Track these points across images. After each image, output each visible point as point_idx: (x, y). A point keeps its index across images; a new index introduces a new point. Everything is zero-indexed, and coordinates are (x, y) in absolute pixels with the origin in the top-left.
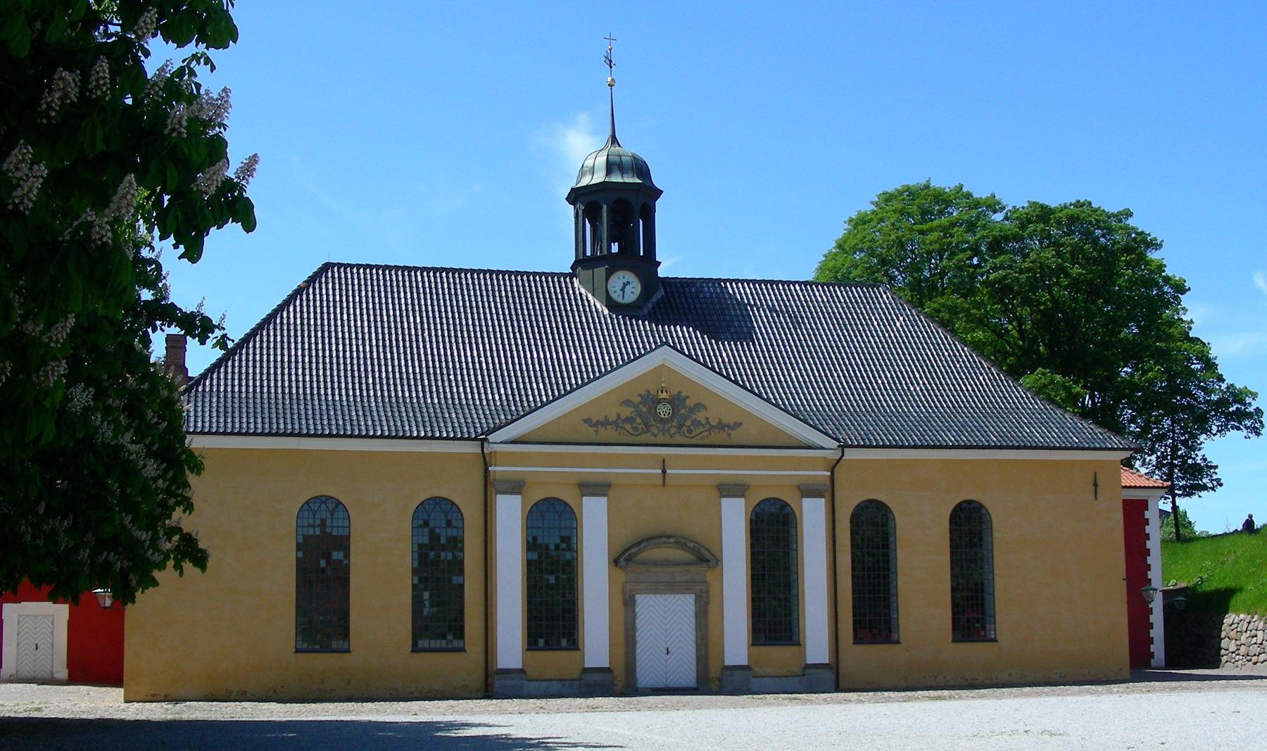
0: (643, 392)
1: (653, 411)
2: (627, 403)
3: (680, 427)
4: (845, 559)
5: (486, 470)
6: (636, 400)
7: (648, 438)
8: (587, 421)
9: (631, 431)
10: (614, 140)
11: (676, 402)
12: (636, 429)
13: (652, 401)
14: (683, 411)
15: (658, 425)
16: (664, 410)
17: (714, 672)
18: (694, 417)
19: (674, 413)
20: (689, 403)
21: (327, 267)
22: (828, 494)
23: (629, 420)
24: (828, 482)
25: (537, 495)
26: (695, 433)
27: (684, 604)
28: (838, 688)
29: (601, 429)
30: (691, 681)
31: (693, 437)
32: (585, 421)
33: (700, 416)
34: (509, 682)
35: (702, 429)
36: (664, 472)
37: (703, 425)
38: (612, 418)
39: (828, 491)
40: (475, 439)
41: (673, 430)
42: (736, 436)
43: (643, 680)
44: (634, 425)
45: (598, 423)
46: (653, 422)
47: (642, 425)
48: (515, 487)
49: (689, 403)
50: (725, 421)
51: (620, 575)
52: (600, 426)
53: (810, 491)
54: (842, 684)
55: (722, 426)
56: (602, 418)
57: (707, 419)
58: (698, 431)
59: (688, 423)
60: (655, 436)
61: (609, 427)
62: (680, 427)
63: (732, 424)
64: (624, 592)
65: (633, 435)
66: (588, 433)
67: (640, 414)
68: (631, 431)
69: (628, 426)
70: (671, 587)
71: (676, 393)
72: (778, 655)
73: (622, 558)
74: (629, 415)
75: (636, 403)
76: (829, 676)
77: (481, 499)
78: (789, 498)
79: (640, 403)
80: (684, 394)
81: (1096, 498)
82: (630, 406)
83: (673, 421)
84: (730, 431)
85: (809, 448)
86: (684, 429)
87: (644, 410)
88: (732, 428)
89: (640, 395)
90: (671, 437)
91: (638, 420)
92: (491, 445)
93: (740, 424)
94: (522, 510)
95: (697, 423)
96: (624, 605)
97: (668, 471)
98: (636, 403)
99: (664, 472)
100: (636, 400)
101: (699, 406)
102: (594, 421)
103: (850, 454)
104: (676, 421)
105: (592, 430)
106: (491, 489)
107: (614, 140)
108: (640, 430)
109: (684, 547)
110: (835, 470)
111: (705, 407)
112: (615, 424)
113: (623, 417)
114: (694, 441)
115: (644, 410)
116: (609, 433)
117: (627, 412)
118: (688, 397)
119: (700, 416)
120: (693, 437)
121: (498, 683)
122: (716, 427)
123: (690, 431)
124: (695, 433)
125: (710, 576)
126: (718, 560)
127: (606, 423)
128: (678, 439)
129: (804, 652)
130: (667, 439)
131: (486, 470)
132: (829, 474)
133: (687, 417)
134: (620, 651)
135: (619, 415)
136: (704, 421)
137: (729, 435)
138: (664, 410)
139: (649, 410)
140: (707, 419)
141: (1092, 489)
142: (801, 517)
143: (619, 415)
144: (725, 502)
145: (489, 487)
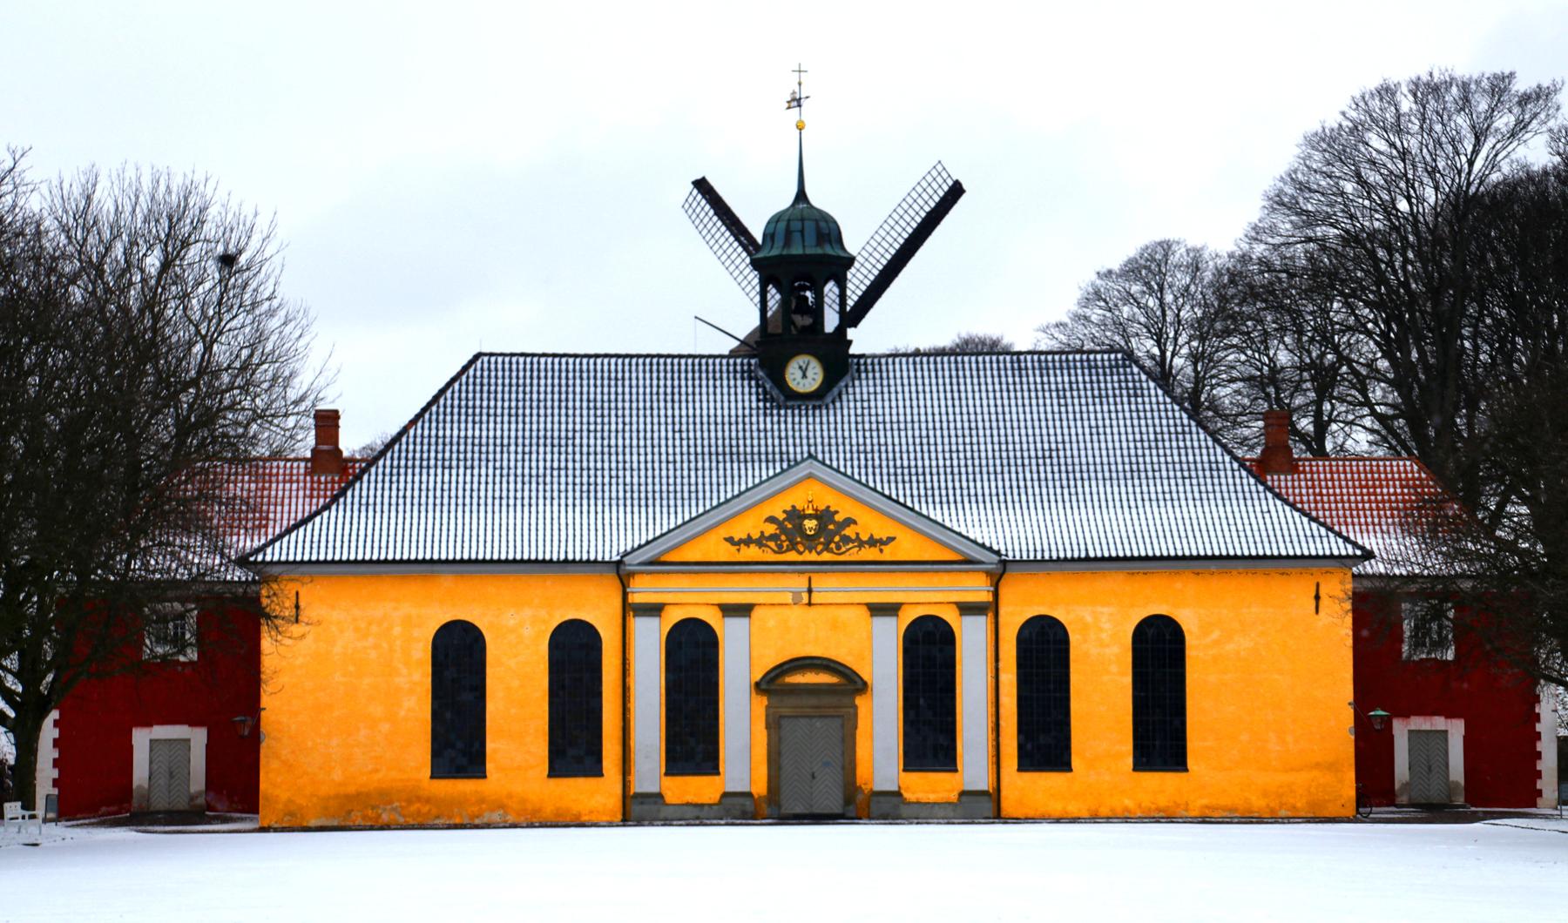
0: (789, 508)
1: (800, 529)
2: (771, 520)
4: (1009, 678)
5: (625, 595)
6: (781, 517)
7: (792, 556)
8: (730, 540)
10: (801, 196)
11: (824, 516)
12: (780, 547)
13: (795, 515)
19: (821, 529)
20: (839, 518)
23: (773, 537)
24: (991, 599)
26: (843, 549)
28: (997, 815)
33: (849, 532)
34: (645, 807)
35: (851, 545)
38: (756, 536)
39: (989, 609)
42: (888, 554)
45: (741, 541)
48: (655, 610)
49: (839, 518)
50: (877, 537)
53: (966, 609)
54: (1003, 813)
55: (873, 542)
56: (744, 536)
57: (857, 534)
59: (837, 539)
65: (775, 552)
69: (772, 544)
71: (822, 507)
76: (988, 806)
77: (620, 621)
78: (950, 616)
80: (832, 509)
81: (1317, 612)
86: (833, 546)
87: (790, 526)
89: (785, 512)
90: (819, 553)
91: (783, 538)
93: (894, 539)
95: (846, 540)
96: (768, 727)
100: (781, 517)
101: (849, 522)
105: (734, 548)
107: (801, 196)
111: (855, 522)
113: (767, 534)
116: (752, 553)
117: (771, 529)
118: (837, 512)
119: (849, 532)
121: (636, 809)
122: (866, 542)
123: (839, 548)
124: (843, 549)
125: (859, 701)
127: (748, 541)
128: (826, 556)
130: (813, 557)
131: (625, 595)
133: (836, 533)
135: (762, 533)
136: (854, 537)
137: (881, 551)
138: (810, 525)
140: (857, 534)
141: (1313, 602)
143: (762, 533)
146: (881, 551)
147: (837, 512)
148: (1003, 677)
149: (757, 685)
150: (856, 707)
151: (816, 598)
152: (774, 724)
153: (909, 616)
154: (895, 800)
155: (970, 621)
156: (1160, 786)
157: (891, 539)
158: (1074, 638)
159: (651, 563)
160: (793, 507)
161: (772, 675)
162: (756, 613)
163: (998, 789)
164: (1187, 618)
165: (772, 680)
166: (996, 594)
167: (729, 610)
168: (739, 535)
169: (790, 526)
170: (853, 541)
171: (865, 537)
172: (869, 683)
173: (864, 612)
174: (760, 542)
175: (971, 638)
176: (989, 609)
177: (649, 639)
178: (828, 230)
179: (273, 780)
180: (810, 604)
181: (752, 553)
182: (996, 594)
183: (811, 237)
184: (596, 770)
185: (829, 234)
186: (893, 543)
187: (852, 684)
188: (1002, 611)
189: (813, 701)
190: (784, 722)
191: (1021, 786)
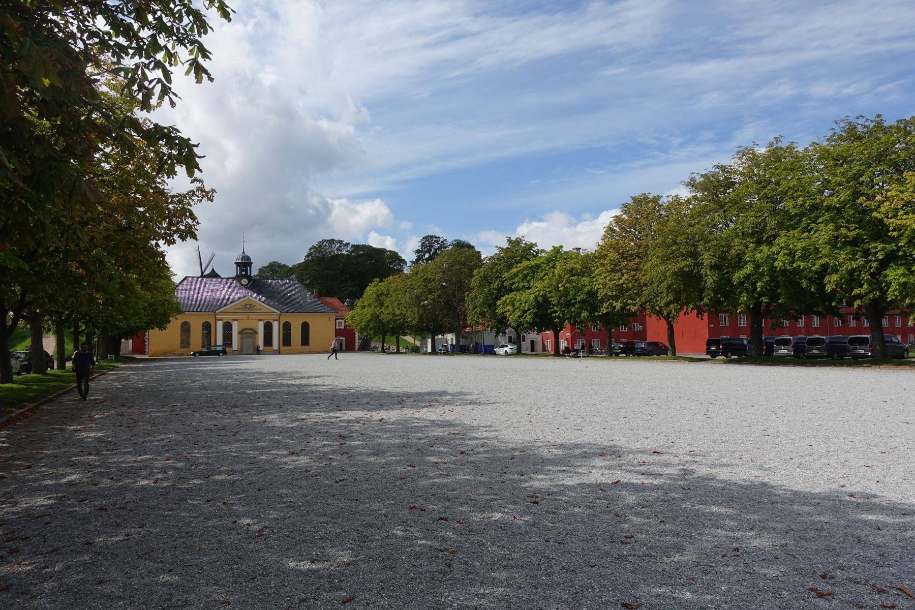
10: (244, 253)
21: (186, 277)
25: (224, 321)
28: (279, 354)
33: (255, 307)
39: (279, 320)
42: (262, 311)
48: (221, 320)
55: (259, 309)
66: (234, 311)
72: (268, 348)
73: (240, 332)
78: (271, 321)
107: (244, 253)
116: (238, 311)
117: (241, 307)
119: (255, 307)
134: (240, 347)
144: (260, 322)
145: (216, 320)
152: (242, 339)
153: (265, 321)
156: (305, 348)
167: (234, 320)
175: (275, 325)
177: (220, 325)
178: (248, 258)
181: (238, 311)
183: (246, 259)
187: (256, 332)
191: (283, 348)
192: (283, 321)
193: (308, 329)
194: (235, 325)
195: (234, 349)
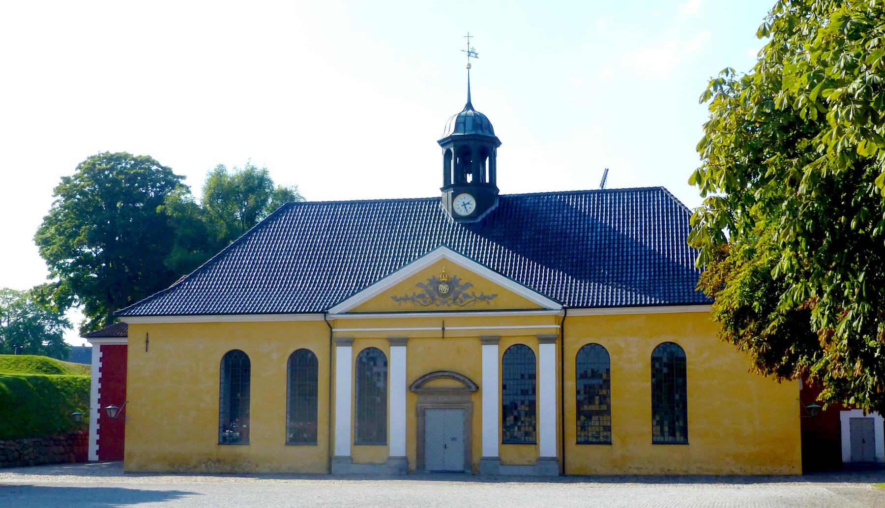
0: (431, 277)
2: (420, 285)
3: (455, 299)
4: (571, 385)
5: (331, 332)
6: (426, 283)
7: (434, 308)
8: (395, 298)
9: (422, 303)
12: (425, 301)
13: (435, 282)
14: (457, 289)
15: (441, 298)
16: (444, 288)
17: (476, 459)
18: (464, 292)
19: (451, 290)
20: (461, 283)
22: (559, 341)
23: (421, 296)
24: (559, 333)
25: (362, 346)
26: (464, 303)
27: (456, 417)
29: (403, 304)
30: (459, 467)
31: (463, 306)
32: (392, 297)
33: (468, 291)
35: (469, 300)
36: (443, 329)
37: (470, 297)
38: (410, 294)
40: (322, 312)
41: (450, 302)
42: (492, 304)
43: (432, 464)
44: (425, 299)
45: (401, 299)
46: (437, 297)
47: (430, 299)
48: (349, 342)
49: (461, 283)
51: (415, 398)
52: (402, 301)
53: (545, 339)
54: (569, 471)
55: (483, 298)
56: (403, 296)
58: (467, 301)
59: (461, 296)
60: (438, 306)
61: (408, 301)
62: (455, 299)
63: (490, 296)
64: (417, 409)
66: (391, 305)
67: (428, 291)
68: (422, 303)
69: (420, 300)
70: (448, 406)
73: (416, 387)
74: (421, 293)
75: (426, 285)
77: (328, 350)
78: (531, 344)
79: (428, 285)
80: (458, 278)
82: (422, 287)
83: (450, 295)
84: (489, 301)
85: (545, 309)
86: (458, 300)
88: (490, 298)
90: (449, 306)
91: (427, 296)
92: (331, 316)
94: (352, 355)
95: (467, 296)
96: (417, 415)
97: (446, 328)
98: (426, 285)
99: (443, 329)
101: (468, 285)
102: (398, 298)
103: (571, 312)
104: (452, 295)
105: (396, 303)
106: (334, 344)
108: (429, 302)
109: (454, 378)
110: (564, 323)
111: (472, 285)
112: (412, 299)
113: (417, 294)
114: (463, 308)
115: (431, 289)
117: (419, 291)
118: (461, 279)
119: (468, 291)
120: (463, 306)
123: (462, 301)
125: (474, 398)
126: (478, 388)
127: (406, 299)
128: (454, 307)
129: (538, 450)
130: (446, 308)
132: (559, 327)
135: (414, 293)
136: (471, 295)
137: (488, 303)
139: (434, 289)
140: (474, 293)
142: (539, 356)
143: (414, 293)
145: (333, 341)
146: (488, 303)
147: (461, 279)
148: (567, 383)
149: (410, 387)
150: (472, 403)
151: (446, 335)
154: (497, 463)
155: (543, 347)
157: (495, 296)
158: (613, 358)
159: (347, 313)
160: (434, 276)
161: (420, 381)
162: (410, 344)
163: (564, 457)
164: (684, 343)
165: (417, 387)
166: (562, 329)
168: (400, 294)
169: (431, 289)
170: (470, 297)
171: (478, 295)
172: (480, 387)
173: (477, 342)
174: (412, 299)
176: (560, 339)
177: (345, 359)
179: (130, 445)
180: (443, 338)
181: (408, 305)
182: (562, 329)
184: (312, 440)
185: (481, 125)
186: (496, 298)
188: (566, 340)
189: (445, 399)
190: (428, 413)
191: (578, 455)
192: (573, 347)
193: (683, 373)
194: (397, 357)
195: (393, 453)
